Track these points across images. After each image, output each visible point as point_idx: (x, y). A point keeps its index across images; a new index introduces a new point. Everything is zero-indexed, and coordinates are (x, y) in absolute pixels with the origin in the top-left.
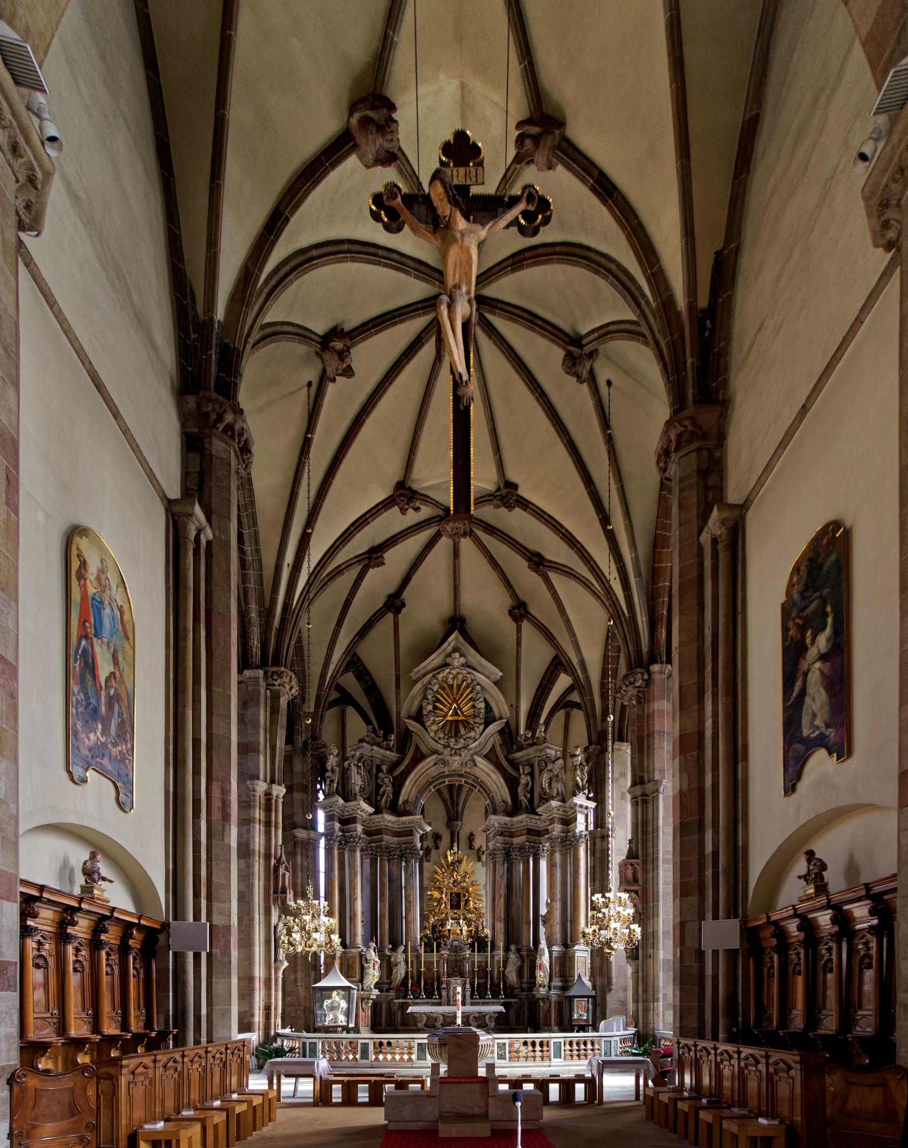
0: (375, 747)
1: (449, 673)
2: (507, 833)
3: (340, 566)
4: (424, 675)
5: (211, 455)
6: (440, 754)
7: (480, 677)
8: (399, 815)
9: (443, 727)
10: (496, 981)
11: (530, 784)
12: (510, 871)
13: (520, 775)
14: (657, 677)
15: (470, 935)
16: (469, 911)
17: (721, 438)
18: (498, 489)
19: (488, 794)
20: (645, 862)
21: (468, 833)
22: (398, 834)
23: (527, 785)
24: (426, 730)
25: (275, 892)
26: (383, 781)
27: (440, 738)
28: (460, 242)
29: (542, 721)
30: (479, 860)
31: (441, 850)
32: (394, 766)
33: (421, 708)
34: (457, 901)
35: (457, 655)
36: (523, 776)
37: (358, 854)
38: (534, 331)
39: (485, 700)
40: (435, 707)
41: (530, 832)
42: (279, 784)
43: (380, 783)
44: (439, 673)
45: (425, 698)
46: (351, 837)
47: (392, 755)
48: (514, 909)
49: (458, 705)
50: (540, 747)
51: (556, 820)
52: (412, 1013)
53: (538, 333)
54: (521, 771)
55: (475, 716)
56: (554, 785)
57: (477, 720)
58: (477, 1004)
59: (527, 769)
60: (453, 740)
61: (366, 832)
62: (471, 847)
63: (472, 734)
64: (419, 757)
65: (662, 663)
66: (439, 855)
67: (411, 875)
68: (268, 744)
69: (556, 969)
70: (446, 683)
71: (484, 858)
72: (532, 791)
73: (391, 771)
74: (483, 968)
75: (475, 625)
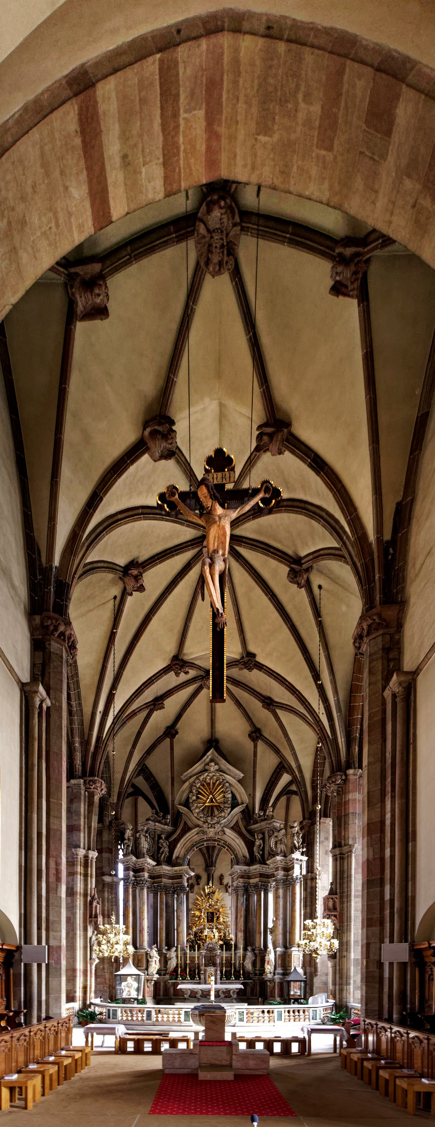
0: (157, 824)
1: (208, 775)
2: (245, 876)
3: (134, 710)
4: (191, 777)
5: (50, 652)
6: (201, 827)
7: (228, 777)
8: (173, 866)
9: (203, 810)
10: (237, 969)
12: (248, 900)
13: (255, 839)
14: (351, 778)
15: (220, 939)
16: (220, 924)
17: (400, 626)
18: (242, 658)
19: (233, 851)
20: (341, 897)
21: (219, 874)
22: (172, 878)
23: (260, 845)
25: (90, 917)
26: (162, 845)
27: (201, 817)
28: (218, 523)
29: (270, 805)
30: (227, 891)
31: (201, 886)
32: (169, 835)
33: (188, 798)
34: (211, 917)
35: (213, 764)
36: (257, 840)
37: (145, 891)
38: (268, 556)
39: (232, 793)
40: (198, 798)
41: (262, 875)
42: (94, 850)
43: (160, 846)
45: (191, 792)
46: (141, 880)
47: (168, 828)
48: (250, 924)
49: (213, 796)
50: (269, 822)
51: (280, 868)
52: (181, 989)
53: (271, 557)
54: (256, 837)
55: (225, 803)
56: (279, 846)
57: (226, 805)
58: (225, 983)
59: (260, 836)
60: (210, 818)
61: (150, 877)
62: (221, 883)
63: (223, 814)
64: (187, 829)
65: (355, 768)
66: (200, 889)
67: (181, 903)
68: (86, 826)
69: (279, 962)
70: (205, 782)
71: (230, 890)
72: (263, 850)
73: (167, 838)
74: (229, 961)
75: (226, 744)
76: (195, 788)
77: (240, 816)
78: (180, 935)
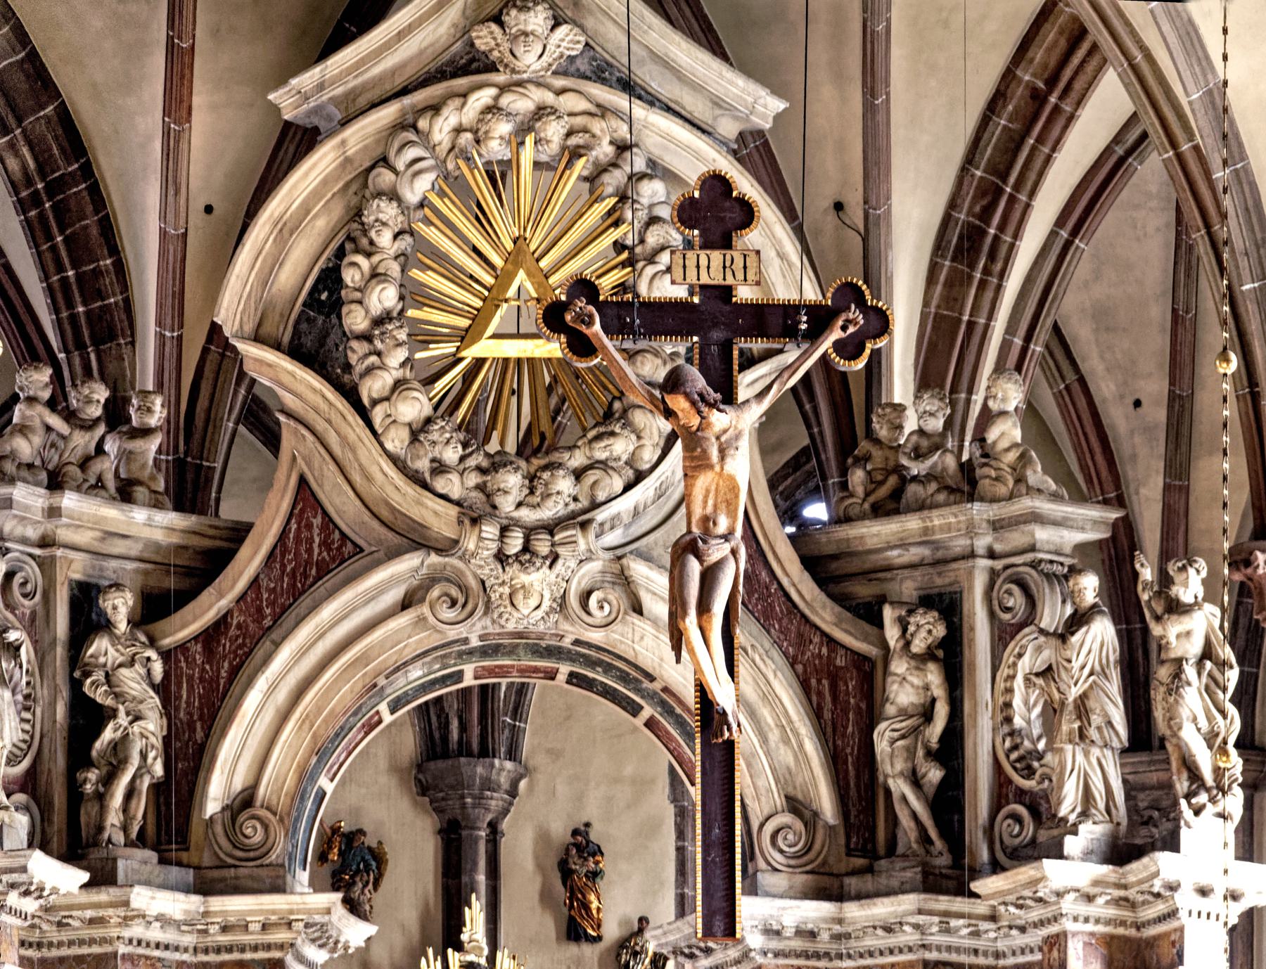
1: (492, 109)
11: (942, 712)
23: (927, 714)
24: (364, 413)
27: (440, 468)
36: (899, 666)
40: (412, 294)
43: (100, 696)
44: (435, 108)
76: (388, 211)
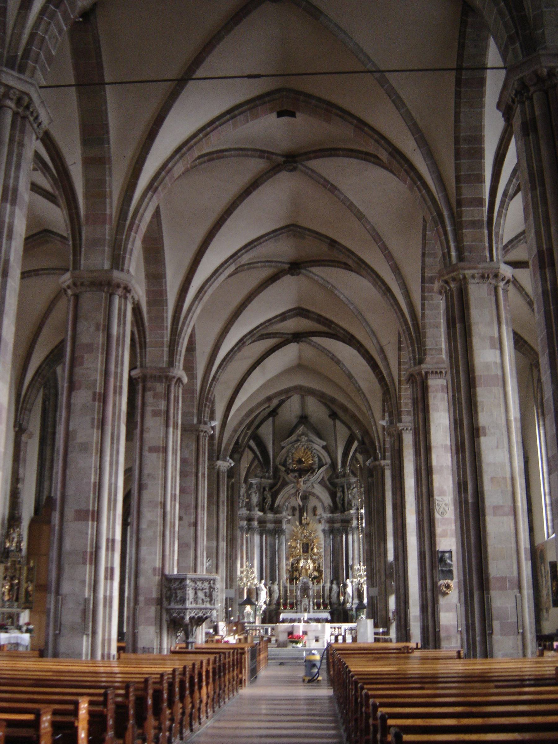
29: (348, 464)
32: (272, 487)
33: (285, 460)
39: (319, 456)
43: (265, 496)
59: (341, 489)
72: (343, 500)
77: (324, 473)
78: (281, 571)
